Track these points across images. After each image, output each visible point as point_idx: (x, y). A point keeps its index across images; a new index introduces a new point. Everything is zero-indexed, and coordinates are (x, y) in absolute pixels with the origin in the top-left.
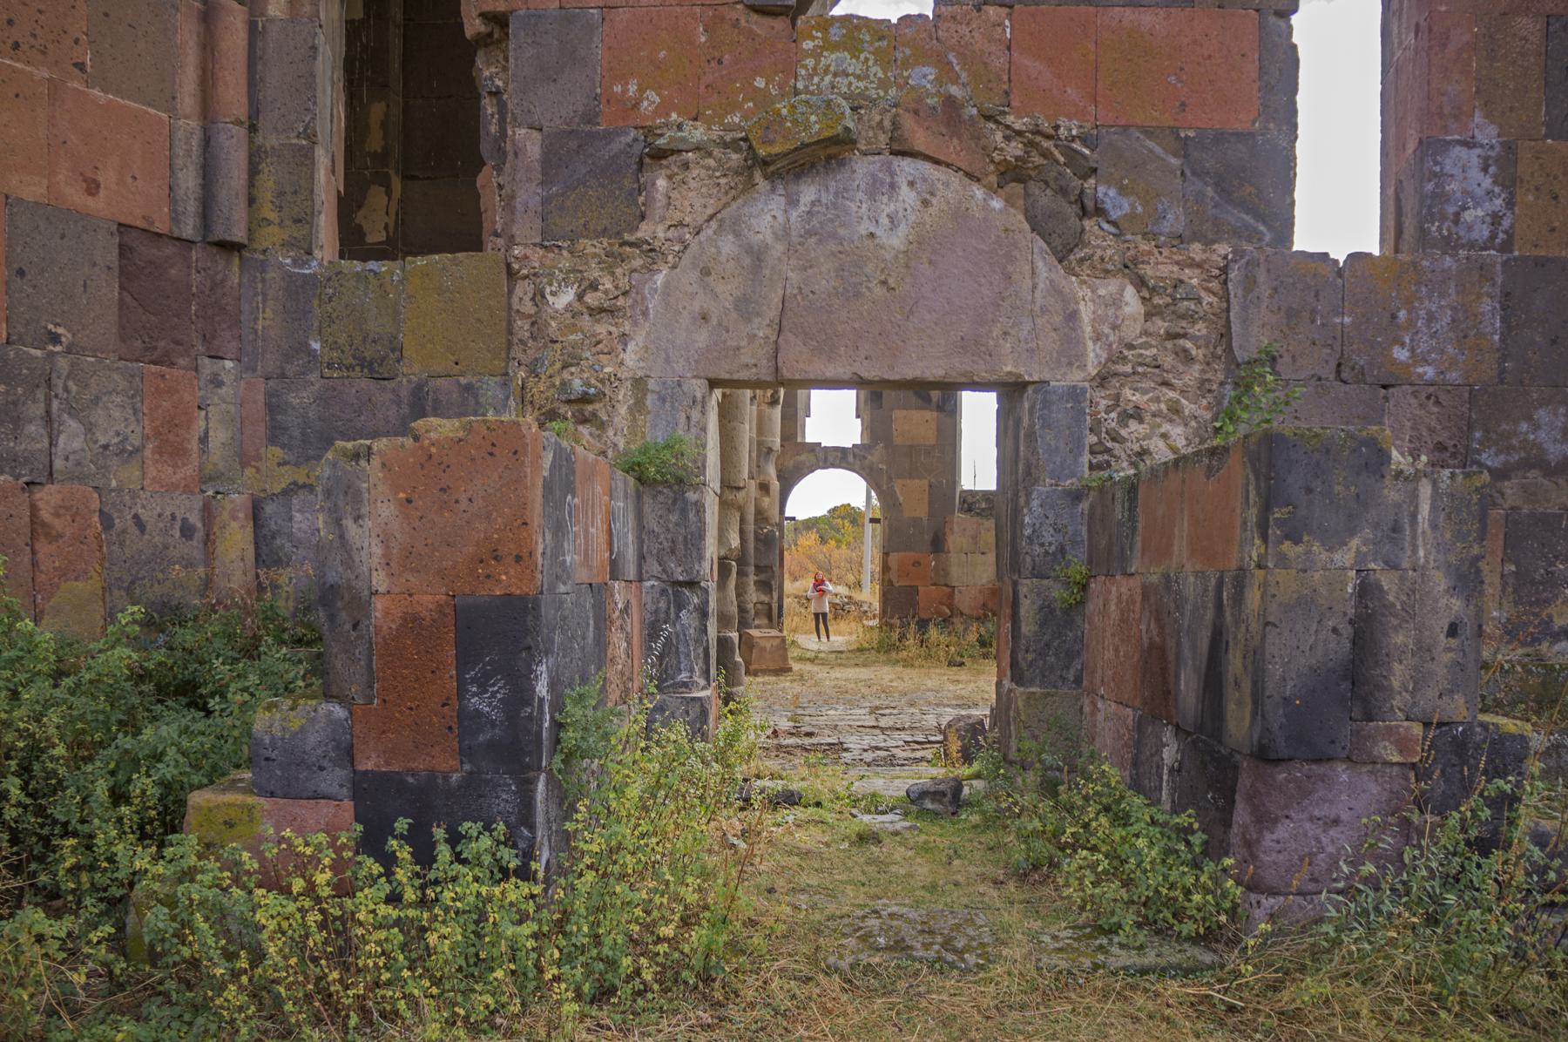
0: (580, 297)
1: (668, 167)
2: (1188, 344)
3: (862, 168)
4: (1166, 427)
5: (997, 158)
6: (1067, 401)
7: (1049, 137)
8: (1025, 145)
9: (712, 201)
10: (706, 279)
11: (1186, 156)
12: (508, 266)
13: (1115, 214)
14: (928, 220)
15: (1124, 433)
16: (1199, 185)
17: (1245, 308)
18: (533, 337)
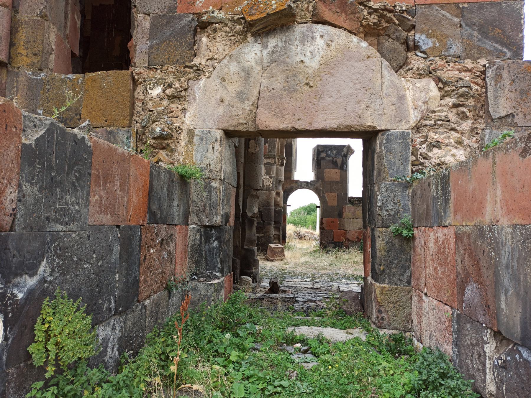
0: (164, 91)
1: (207, 32)
2: (465, 110)
3: (299, 29)
4: (454, 151)
5: (364, 23)
6: (400, 139)
7: (390, 11)
8: (378, 17)
9: (228, 48)
10: (223, 83)
11: (463, 16)
12: (133, 78)
13: (424, 48)
14: (329, 53)
15: (430, 154)
16: (470, 30)
17: (495, 91)
18: (143, 110)
